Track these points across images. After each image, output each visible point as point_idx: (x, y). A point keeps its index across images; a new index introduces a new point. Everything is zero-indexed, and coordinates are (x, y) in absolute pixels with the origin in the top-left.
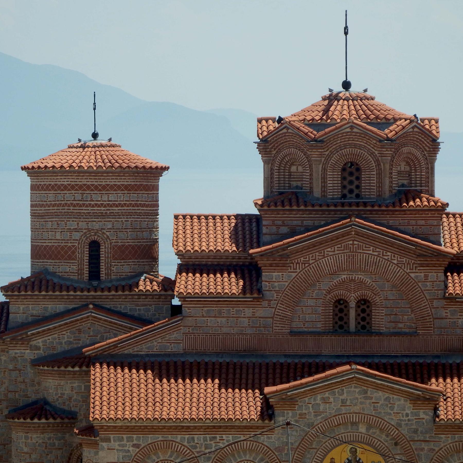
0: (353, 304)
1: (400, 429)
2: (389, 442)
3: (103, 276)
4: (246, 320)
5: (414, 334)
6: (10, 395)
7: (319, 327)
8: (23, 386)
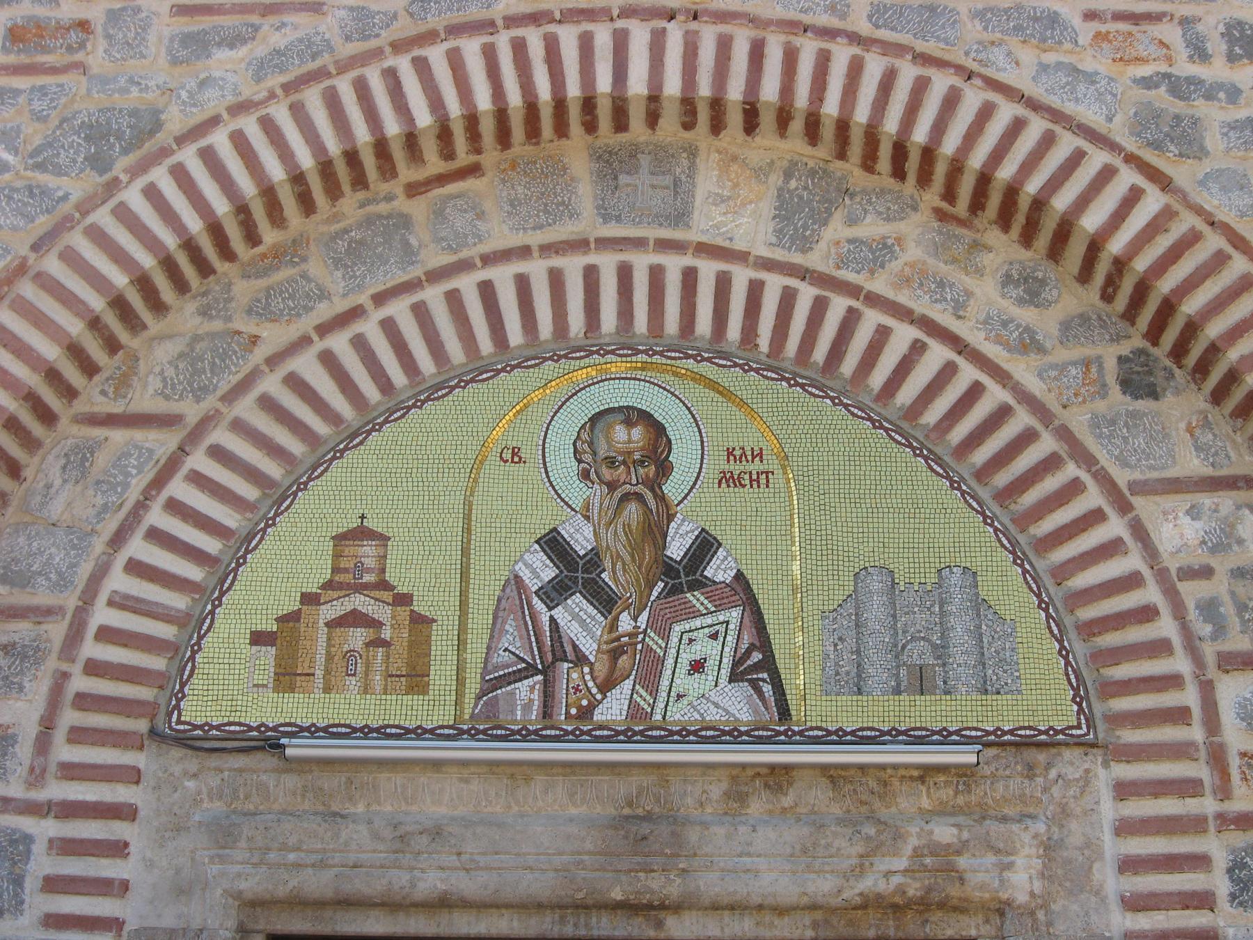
1: (1182, 173)
2: (1063, 355)
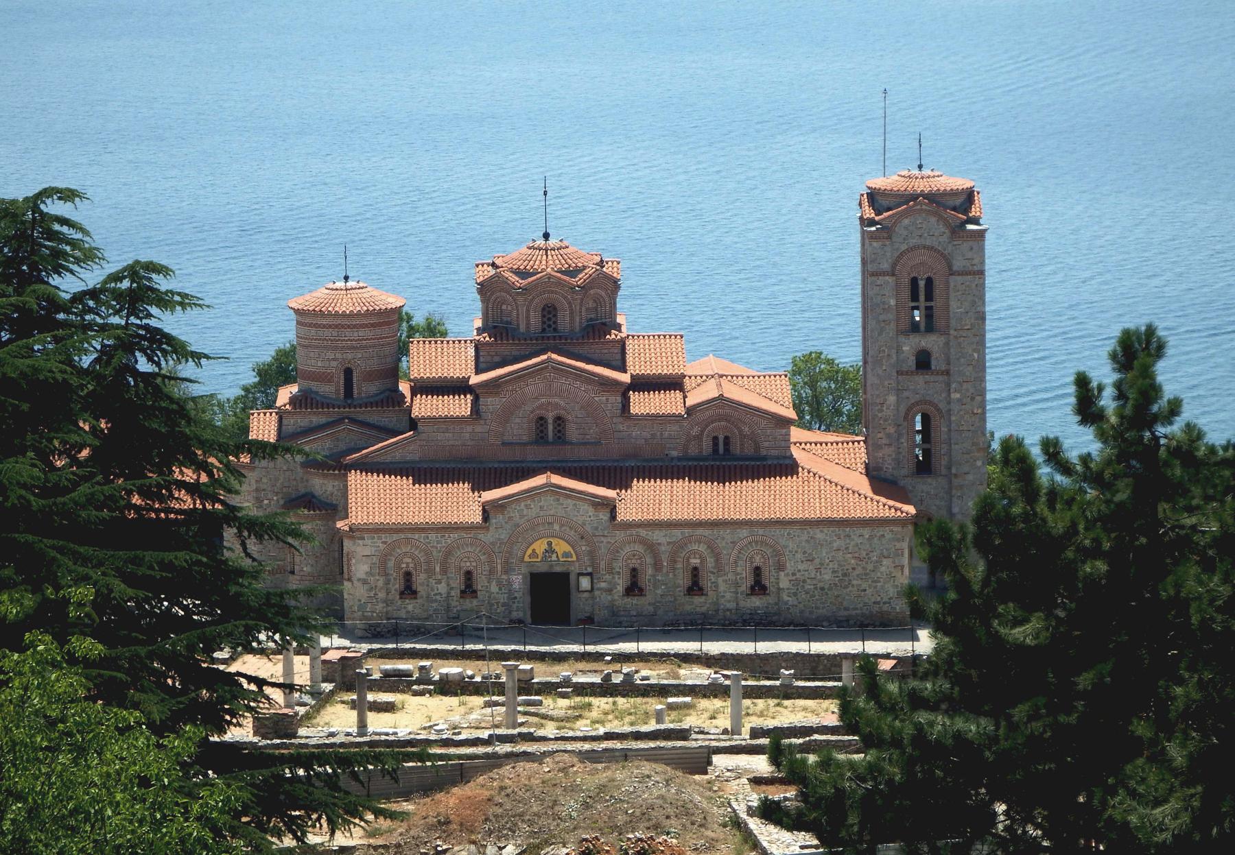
0: (550, 421)
3: (355, 395)
4: (468, 435)
5: (597, 443)
6: (284, 490)
7: (525, 438)
8: (295, 483)
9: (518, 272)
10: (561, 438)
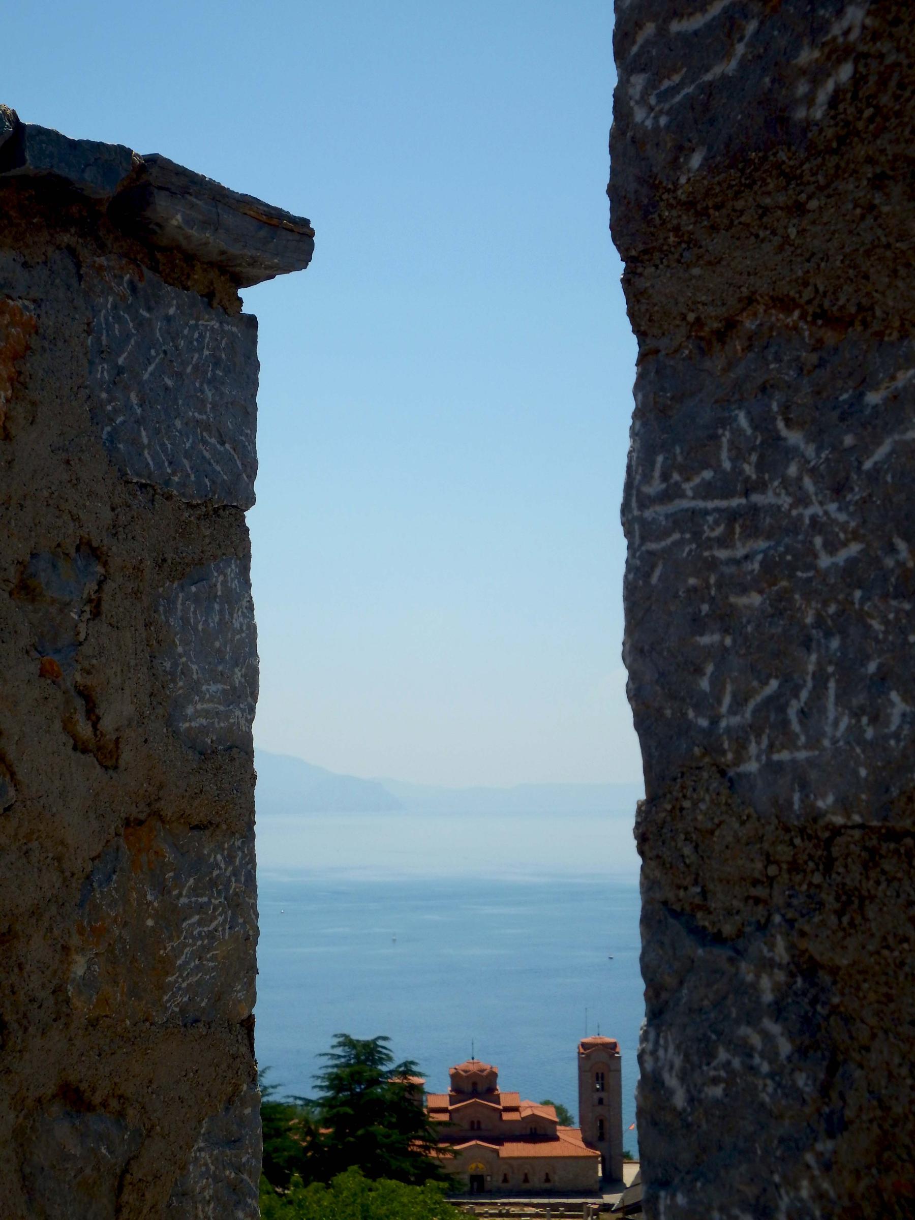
9: (465, 1071)
10: (479, 1128)
